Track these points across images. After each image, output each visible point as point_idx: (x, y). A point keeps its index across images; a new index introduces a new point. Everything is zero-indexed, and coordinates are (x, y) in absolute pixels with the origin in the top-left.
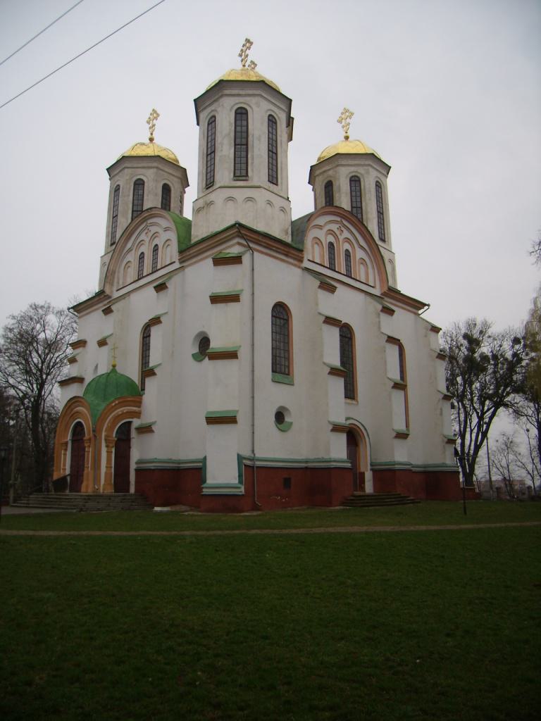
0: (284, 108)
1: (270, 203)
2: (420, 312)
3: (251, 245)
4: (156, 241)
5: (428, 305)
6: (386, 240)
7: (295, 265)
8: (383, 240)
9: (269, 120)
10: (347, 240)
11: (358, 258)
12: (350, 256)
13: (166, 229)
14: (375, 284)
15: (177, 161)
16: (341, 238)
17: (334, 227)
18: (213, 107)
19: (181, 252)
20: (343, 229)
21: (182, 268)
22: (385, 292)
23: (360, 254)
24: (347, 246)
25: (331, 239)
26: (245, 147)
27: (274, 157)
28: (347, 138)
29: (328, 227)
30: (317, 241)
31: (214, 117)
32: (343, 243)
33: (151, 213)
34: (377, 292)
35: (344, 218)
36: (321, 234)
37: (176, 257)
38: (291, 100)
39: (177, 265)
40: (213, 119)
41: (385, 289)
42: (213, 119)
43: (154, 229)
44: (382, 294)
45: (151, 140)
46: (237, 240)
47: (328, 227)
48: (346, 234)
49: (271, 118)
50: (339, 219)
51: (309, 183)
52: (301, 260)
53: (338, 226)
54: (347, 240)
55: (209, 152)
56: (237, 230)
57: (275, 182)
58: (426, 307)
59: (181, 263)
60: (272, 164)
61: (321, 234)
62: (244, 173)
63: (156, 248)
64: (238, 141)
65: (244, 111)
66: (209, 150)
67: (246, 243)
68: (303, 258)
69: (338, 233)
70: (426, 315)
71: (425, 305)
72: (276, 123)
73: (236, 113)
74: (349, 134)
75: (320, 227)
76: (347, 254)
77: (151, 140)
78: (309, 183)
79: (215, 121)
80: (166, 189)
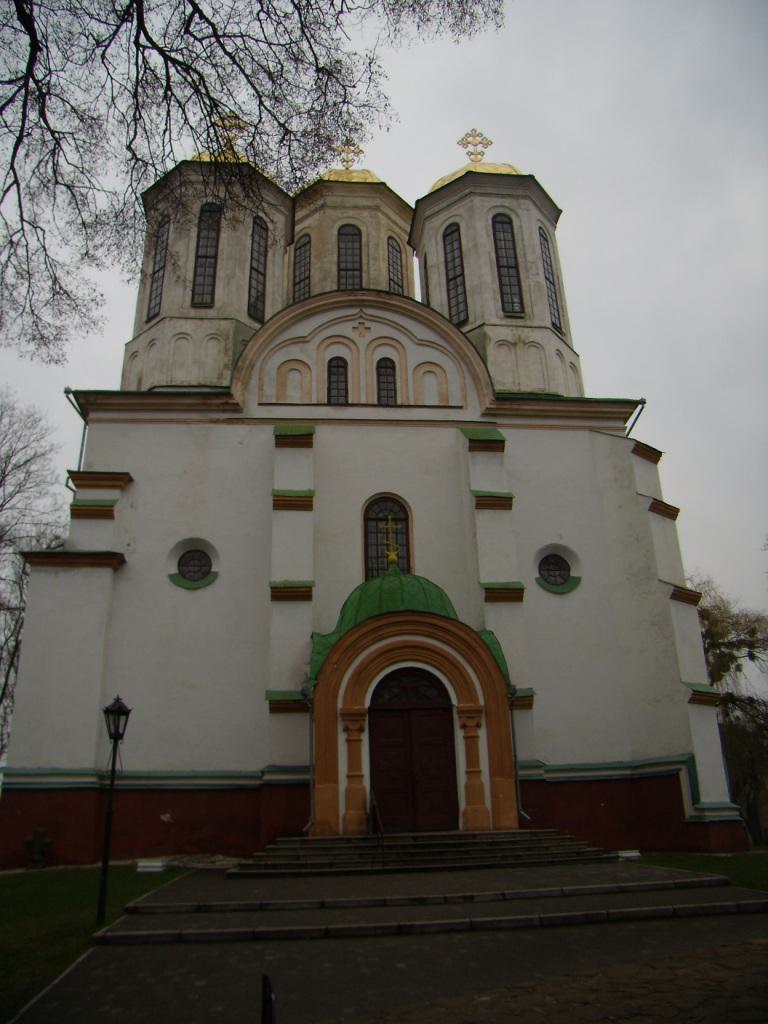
1: (182, 336)
2: (629, 424)
5: (643, 402)
7: (229, 421)
8: (513, 307)
14: (465, 398)
16: (362, 343)
17: (346, 329)
20: (367, 324)
22: (488, 409)
34: (472, 413)
35: (366, 306)
41: (488, 402)
44: (484, 415)
48: (379, 330)
52: (237, 408)
53: (356, 324)
58: (640, 407)
62: (207, 298)
68: (237, 404)
69: (353, 335)
70: (642, 430)
71: (633, 404)
75: (301, 340)
76: (386, 368)
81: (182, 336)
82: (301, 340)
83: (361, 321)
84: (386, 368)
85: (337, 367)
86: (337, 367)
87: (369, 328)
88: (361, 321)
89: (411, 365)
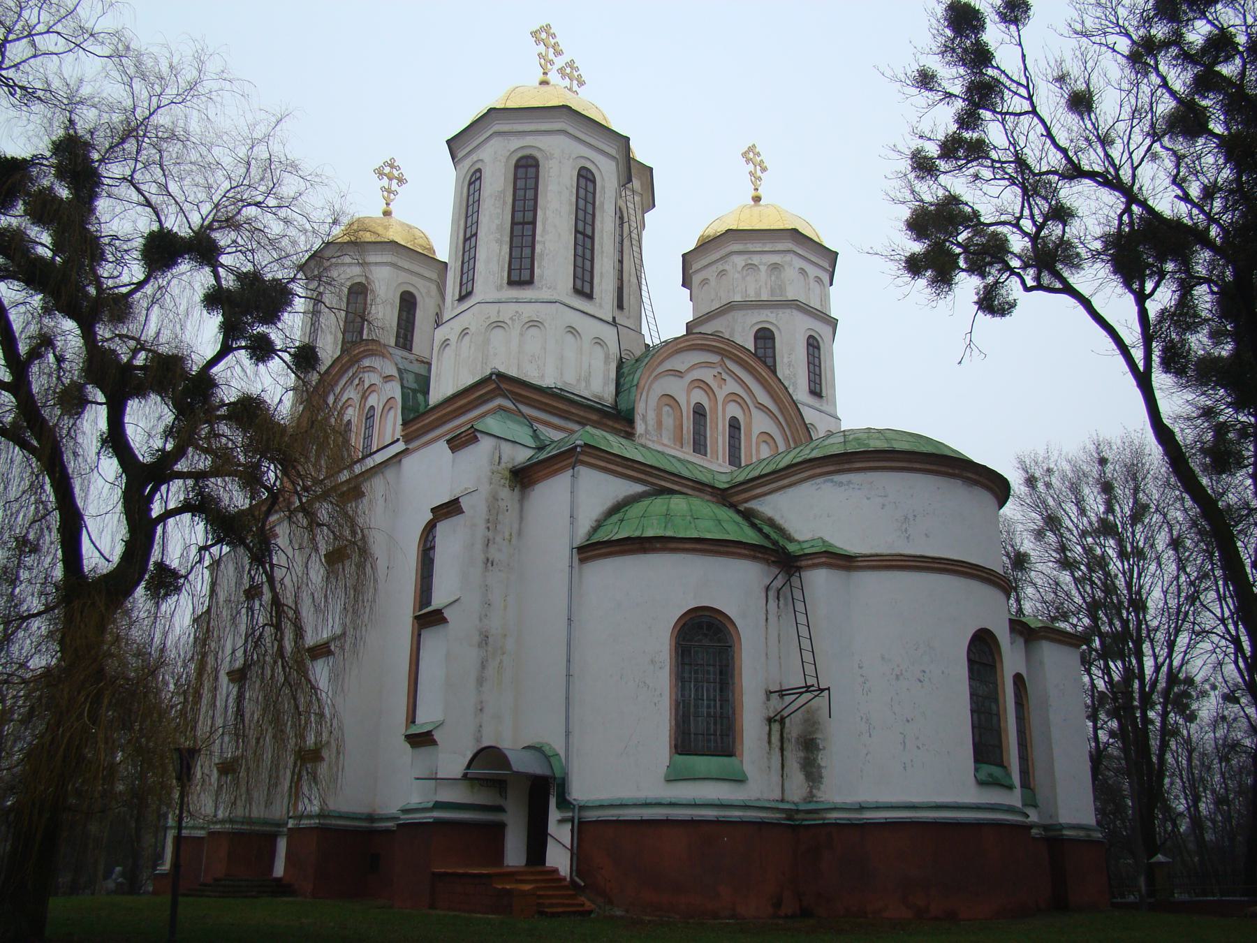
0: (613, 152)
1: (572, 330)
3: (526, 410)
4: (372, 400)
6: (824, 394)
9: (579, 175)
10: (733, 397)
11: (755, 432)
12: (739, 429)
13: (388, 378)
15: (432, 250)
16: (721, 395)
18: (474, 157)
19: (405, 423)
20: (724, 376)
21: (405, 452)
23: (760, 423)
24: (734, 410)
25: (699, 396)
26: (531, 226)
27: (589, 246)
28: (757, 199)
29: (697, 374)
30: (670, 399)
31: (479, 170)
32: (725, 404)
33: (376, 348)
35: (727, 356)
36: (676, 387)
37: (398, 433)
38: (628, 139)
39: (400, 446)
40: (478, 175)
42: (478, 175)
43: (370, 378)
45: (387, 213)
46: (499, 401)
47: (697, 374)
48: (732, 386)
49: (584, 173)
50: (715, 358)
51: (683, 285)
54: (733, 397)
55: (468, 235)
56: (494, 386)
57: (587, 290)
59: (406, 442)
60: (584, 257)
61: (676, 387)
63: (370, 416)
64: (519, 216)
65: (531, 162)
66: (469, 230)
67: (514, 407)
69: (714, 386)
72: (594, 182)
73: (517, 167)
74: (760, 192)
75: (678, 374)
76: (734, 425)
77: (387, 213)
78: (683, 285)
79: (480, 178)
80: (408, 303)
81: (572, 330)
82: (678, 374)
83: (720, 371)
84: (734, 425)
85: (699, 412)
86: (699, 412)
87: (725, 380)
88: (720, 371)
89: (755, 432)
